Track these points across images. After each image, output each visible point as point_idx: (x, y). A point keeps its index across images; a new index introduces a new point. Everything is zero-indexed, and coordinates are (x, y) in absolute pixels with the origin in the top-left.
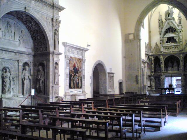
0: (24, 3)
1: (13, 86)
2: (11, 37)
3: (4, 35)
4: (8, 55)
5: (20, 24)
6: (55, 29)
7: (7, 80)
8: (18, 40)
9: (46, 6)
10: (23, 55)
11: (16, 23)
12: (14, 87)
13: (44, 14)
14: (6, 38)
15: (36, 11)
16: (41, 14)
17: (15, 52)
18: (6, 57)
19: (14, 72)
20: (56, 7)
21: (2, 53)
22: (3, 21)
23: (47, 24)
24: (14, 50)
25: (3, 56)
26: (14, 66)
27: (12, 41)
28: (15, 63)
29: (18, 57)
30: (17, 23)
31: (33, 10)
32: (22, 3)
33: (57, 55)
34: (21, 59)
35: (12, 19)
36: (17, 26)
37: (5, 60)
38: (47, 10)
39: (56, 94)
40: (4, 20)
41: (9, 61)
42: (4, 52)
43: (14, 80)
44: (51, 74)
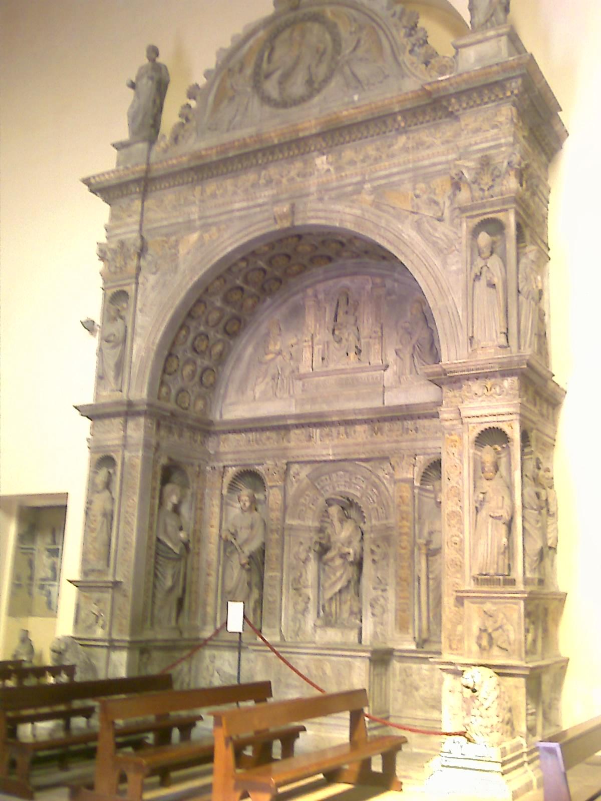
0: (273, 196)
1: (374, 588)
2: (352, 355)
3: (323, 359)
4: (336, 442)
5: (396, 280)
6: (477, 220)
7: (332, 559)
8: (391, 357)
9: (404, 131)
10: (421, 423)
11: (378, 280)
12: (380, 593)
13: (396, 179)
14: (332, 366)
15: (339, 198)
16: (375, 189)
17: (365, 422)
18: (324, 452)
19: (378, 518)
20: (458, 95)
21: (310, 437)
22: (318, 302)
23: (418, 227)
24: (355, 411)
25: (310, 451)
26: (375, 486)
27: (355, 370)
28: (381, 474)
29: (386, 440)
30: (382, 276)
31: (321, 199)
32: (260, 201)
33: (489, 383)
34: (403, 445)
35: (355, 274)
36: (389, 294)
37: (327, 468)
38: (420, 145)
39: (495, 651)
40: (321, 296)
41: (349, 467)
42: (317, 432)
43: (376, 558)
44: (454, 514)
